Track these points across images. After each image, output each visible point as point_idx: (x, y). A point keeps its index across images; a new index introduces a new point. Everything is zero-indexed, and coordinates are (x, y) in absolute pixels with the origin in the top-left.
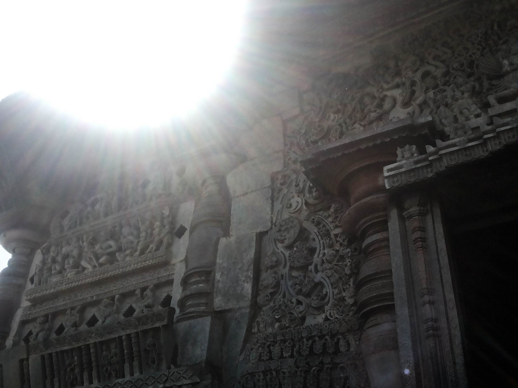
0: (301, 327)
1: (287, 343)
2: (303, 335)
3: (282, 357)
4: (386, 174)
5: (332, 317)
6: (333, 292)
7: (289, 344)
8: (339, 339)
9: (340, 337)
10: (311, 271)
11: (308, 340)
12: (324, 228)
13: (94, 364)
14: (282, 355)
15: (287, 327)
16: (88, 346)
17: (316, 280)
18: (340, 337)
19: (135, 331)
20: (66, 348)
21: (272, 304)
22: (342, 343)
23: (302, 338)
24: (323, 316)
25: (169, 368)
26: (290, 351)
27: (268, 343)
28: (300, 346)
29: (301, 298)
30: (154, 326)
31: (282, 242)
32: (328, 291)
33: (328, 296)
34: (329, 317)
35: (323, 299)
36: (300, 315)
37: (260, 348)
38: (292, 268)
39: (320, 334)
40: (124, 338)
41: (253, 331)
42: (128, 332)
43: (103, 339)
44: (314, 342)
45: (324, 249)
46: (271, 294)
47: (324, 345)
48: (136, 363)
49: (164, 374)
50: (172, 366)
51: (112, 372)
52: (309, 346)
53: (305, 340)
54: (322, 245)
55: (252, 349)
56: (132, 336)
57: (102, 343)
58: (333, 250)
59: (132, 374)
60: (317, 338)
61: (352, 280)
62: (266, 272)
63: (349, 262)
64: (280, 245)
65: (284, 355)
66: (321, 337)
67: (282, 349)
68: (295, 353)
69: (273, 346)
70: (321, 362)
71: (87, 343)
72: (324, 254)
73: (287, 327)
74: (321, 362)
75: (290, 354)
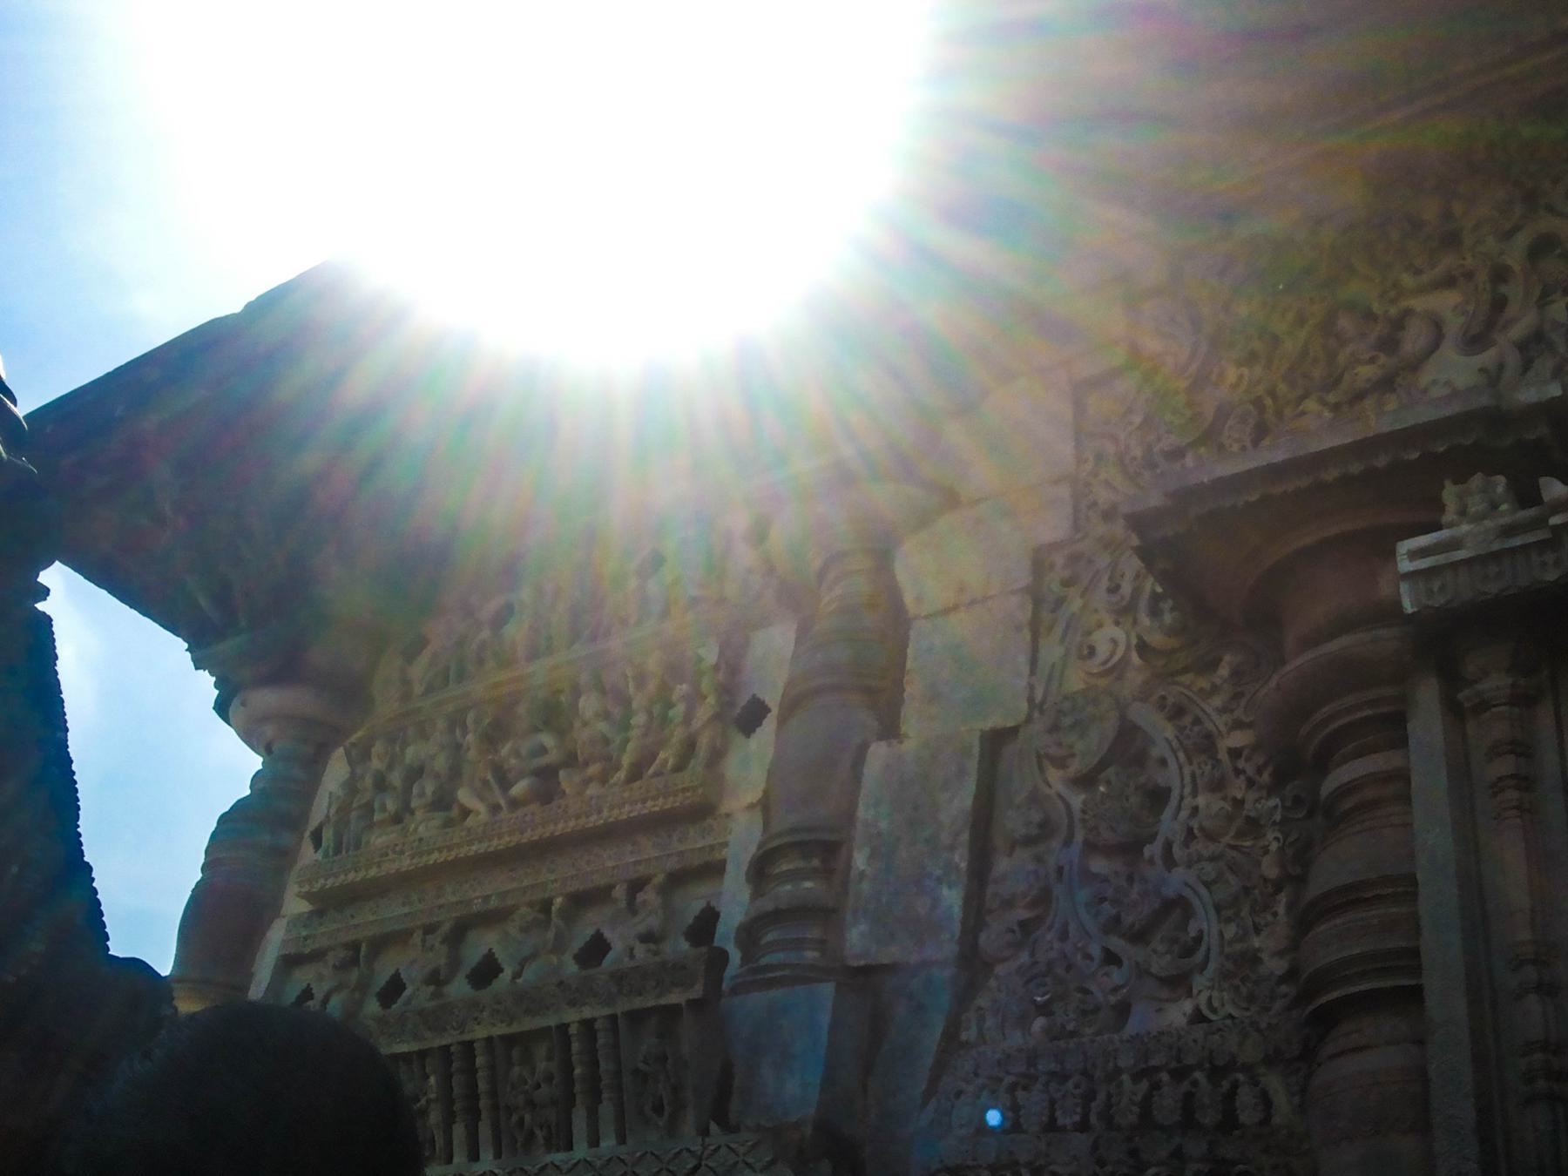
0: (1116, 1037)
1: (1070, 1084)
2: (1122, 1063)
3: (1051, 1126)
4: (1405, 566)
5: (1214, 1011)
6: (1221, 934)
7: (1077, 1086)
8: (1235, 1085)
9: (1241, 1077)
10: (1151, 861)
11: (1137, 1077)
12: (1196, 729)
13: (484, 1103)
14: (1053, 1119)
15: (1073, 1034)
16: (469, 1046)
17: (1169, 892)
18: (1241, 1077)
19: (607, 1011)
20: (404, 1048)
21: (1024, 958)
22: (1245, 1096)
23: (1118, 1071)
24: (1187, 1006)
25: (705, 1132)
26: (1079, 1110)
27: (1009, 1080)
28: (1109, 1096)
29: (1117, 944)
30: (663, 1001)
31: (1061, 763)
32: (1205, 926)
33: (1204, 947)
34: (1206, 1012)
35: (1188, 952)
36: (1113, 999)
37: (985, 1093)
38: (1091, 847)
39: (1174, 1064)
40: (573, 1030)
41: (964, 1036)
42: (587, 1013)
43: (515, 1028)
44: (1156, 1086)
45: (1195, 794)
46: (1023, 924)
47: (1189, 1096)
48: (606, 1109)
49: (688, 1150)
50: (713, 1127)
51: (538, 1132)
52: (1138, 1098)
53: (1125, 1077)
54: (1188, 779)
55: (959, 1094)
56: (597, 1025)
57: (509, 1040)
58: (1224, 799)
59: (594, 1142)
60: (1165, 1077)
61: (1283, 898)
62: (1010, 855)
63: (1277, 839)
64: (1054, 775)
65: (1060, 1122)
66: (1179, 1074)
67: (1052, 1103)
68: (1093, 1119)
69: (1025, 1088)
70: (1178, 1154)
71: (467, 1037)
72: (1195, 810)
73: (1073, 1034)
74: (1178, 1154)
75: (1077, 1118)
